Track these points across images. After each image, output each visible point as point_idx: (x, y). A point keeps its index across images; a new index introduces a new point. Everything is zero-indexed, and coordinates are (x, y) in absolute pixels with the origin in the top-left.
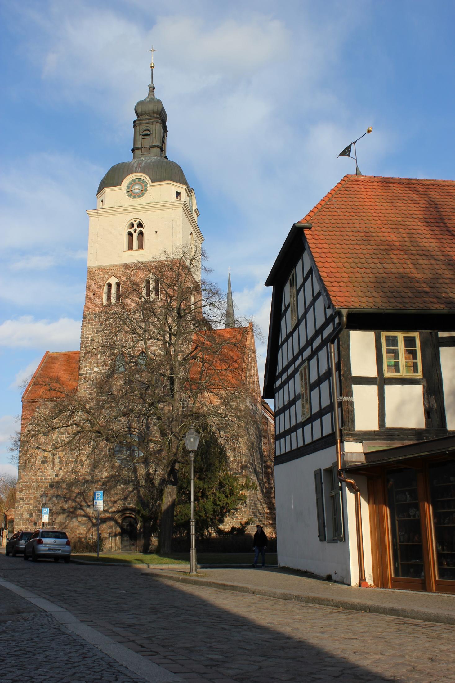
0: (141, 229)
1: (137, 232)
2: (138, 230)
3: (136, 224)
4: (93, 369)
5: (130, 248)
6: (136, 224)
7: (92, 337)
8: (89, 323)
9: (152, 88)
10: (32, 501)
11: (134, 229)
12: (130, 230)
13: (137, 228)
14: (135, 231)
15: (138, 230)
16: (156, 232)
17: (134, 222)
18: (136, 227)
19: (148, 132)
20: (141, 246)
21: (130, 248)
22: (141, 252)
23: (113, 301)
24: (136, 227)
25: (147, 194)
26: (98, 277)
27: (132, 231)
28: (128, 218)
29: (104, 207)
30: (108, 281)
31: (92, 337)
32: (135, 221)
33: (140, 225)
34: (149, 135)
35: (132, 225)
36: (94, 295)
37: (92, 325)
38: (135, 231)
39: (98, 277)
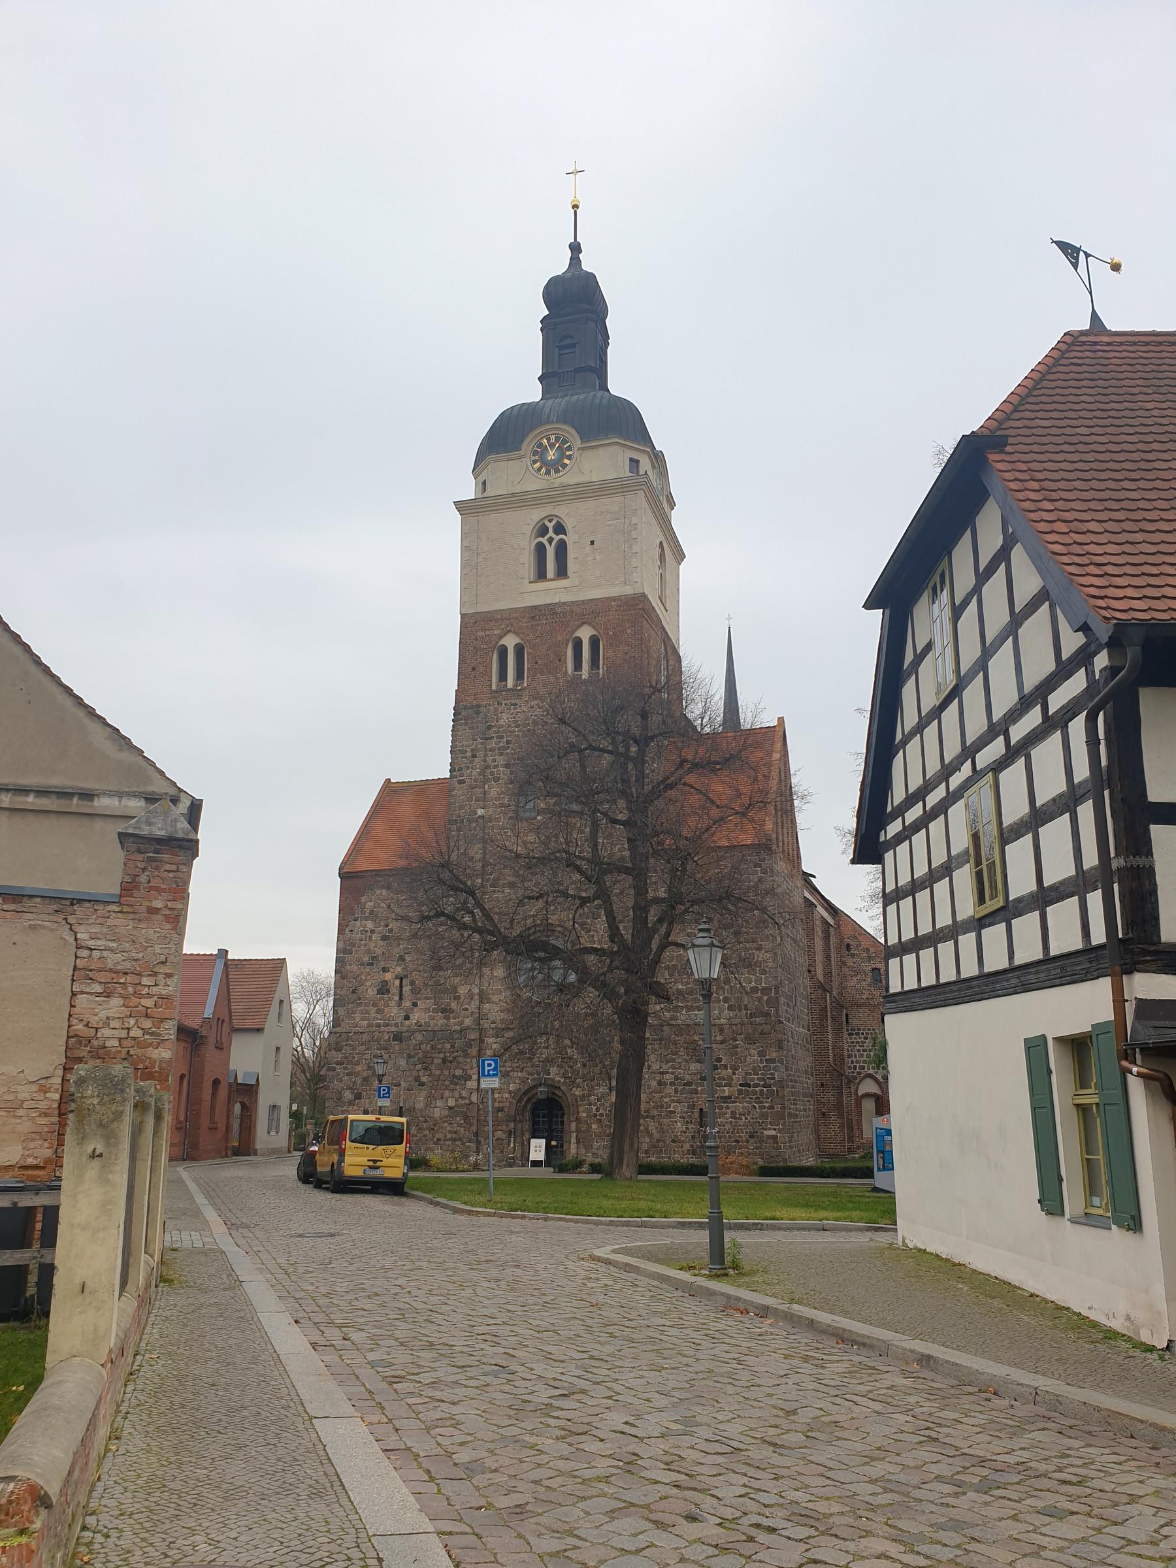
2: (557, 538)
3: (550, 526)
5: (541, 575)
6: (550, 526)
11: (547, 537)
12: (540, 539)
13: (554, 536)
14: (550, 540)
15: (557, 538)
16: (592, 543)
17: (547, 523)
18: (551, 533)
19: (568, 341)
20: (562, 572)
21: (541, 575)
22: (563, 583)
24: (551, 533)
26: (481, 633)
27: (544, 540)
28: (536, 515)
29: (486, 495)
30: (502, 642)
31: (472, 750)
32: (550, 521)
33: (560, 529)
34: (574, 346)
35: (543, 531)
36: (474, 669)
37: (473, 728)
38: (550, 540)
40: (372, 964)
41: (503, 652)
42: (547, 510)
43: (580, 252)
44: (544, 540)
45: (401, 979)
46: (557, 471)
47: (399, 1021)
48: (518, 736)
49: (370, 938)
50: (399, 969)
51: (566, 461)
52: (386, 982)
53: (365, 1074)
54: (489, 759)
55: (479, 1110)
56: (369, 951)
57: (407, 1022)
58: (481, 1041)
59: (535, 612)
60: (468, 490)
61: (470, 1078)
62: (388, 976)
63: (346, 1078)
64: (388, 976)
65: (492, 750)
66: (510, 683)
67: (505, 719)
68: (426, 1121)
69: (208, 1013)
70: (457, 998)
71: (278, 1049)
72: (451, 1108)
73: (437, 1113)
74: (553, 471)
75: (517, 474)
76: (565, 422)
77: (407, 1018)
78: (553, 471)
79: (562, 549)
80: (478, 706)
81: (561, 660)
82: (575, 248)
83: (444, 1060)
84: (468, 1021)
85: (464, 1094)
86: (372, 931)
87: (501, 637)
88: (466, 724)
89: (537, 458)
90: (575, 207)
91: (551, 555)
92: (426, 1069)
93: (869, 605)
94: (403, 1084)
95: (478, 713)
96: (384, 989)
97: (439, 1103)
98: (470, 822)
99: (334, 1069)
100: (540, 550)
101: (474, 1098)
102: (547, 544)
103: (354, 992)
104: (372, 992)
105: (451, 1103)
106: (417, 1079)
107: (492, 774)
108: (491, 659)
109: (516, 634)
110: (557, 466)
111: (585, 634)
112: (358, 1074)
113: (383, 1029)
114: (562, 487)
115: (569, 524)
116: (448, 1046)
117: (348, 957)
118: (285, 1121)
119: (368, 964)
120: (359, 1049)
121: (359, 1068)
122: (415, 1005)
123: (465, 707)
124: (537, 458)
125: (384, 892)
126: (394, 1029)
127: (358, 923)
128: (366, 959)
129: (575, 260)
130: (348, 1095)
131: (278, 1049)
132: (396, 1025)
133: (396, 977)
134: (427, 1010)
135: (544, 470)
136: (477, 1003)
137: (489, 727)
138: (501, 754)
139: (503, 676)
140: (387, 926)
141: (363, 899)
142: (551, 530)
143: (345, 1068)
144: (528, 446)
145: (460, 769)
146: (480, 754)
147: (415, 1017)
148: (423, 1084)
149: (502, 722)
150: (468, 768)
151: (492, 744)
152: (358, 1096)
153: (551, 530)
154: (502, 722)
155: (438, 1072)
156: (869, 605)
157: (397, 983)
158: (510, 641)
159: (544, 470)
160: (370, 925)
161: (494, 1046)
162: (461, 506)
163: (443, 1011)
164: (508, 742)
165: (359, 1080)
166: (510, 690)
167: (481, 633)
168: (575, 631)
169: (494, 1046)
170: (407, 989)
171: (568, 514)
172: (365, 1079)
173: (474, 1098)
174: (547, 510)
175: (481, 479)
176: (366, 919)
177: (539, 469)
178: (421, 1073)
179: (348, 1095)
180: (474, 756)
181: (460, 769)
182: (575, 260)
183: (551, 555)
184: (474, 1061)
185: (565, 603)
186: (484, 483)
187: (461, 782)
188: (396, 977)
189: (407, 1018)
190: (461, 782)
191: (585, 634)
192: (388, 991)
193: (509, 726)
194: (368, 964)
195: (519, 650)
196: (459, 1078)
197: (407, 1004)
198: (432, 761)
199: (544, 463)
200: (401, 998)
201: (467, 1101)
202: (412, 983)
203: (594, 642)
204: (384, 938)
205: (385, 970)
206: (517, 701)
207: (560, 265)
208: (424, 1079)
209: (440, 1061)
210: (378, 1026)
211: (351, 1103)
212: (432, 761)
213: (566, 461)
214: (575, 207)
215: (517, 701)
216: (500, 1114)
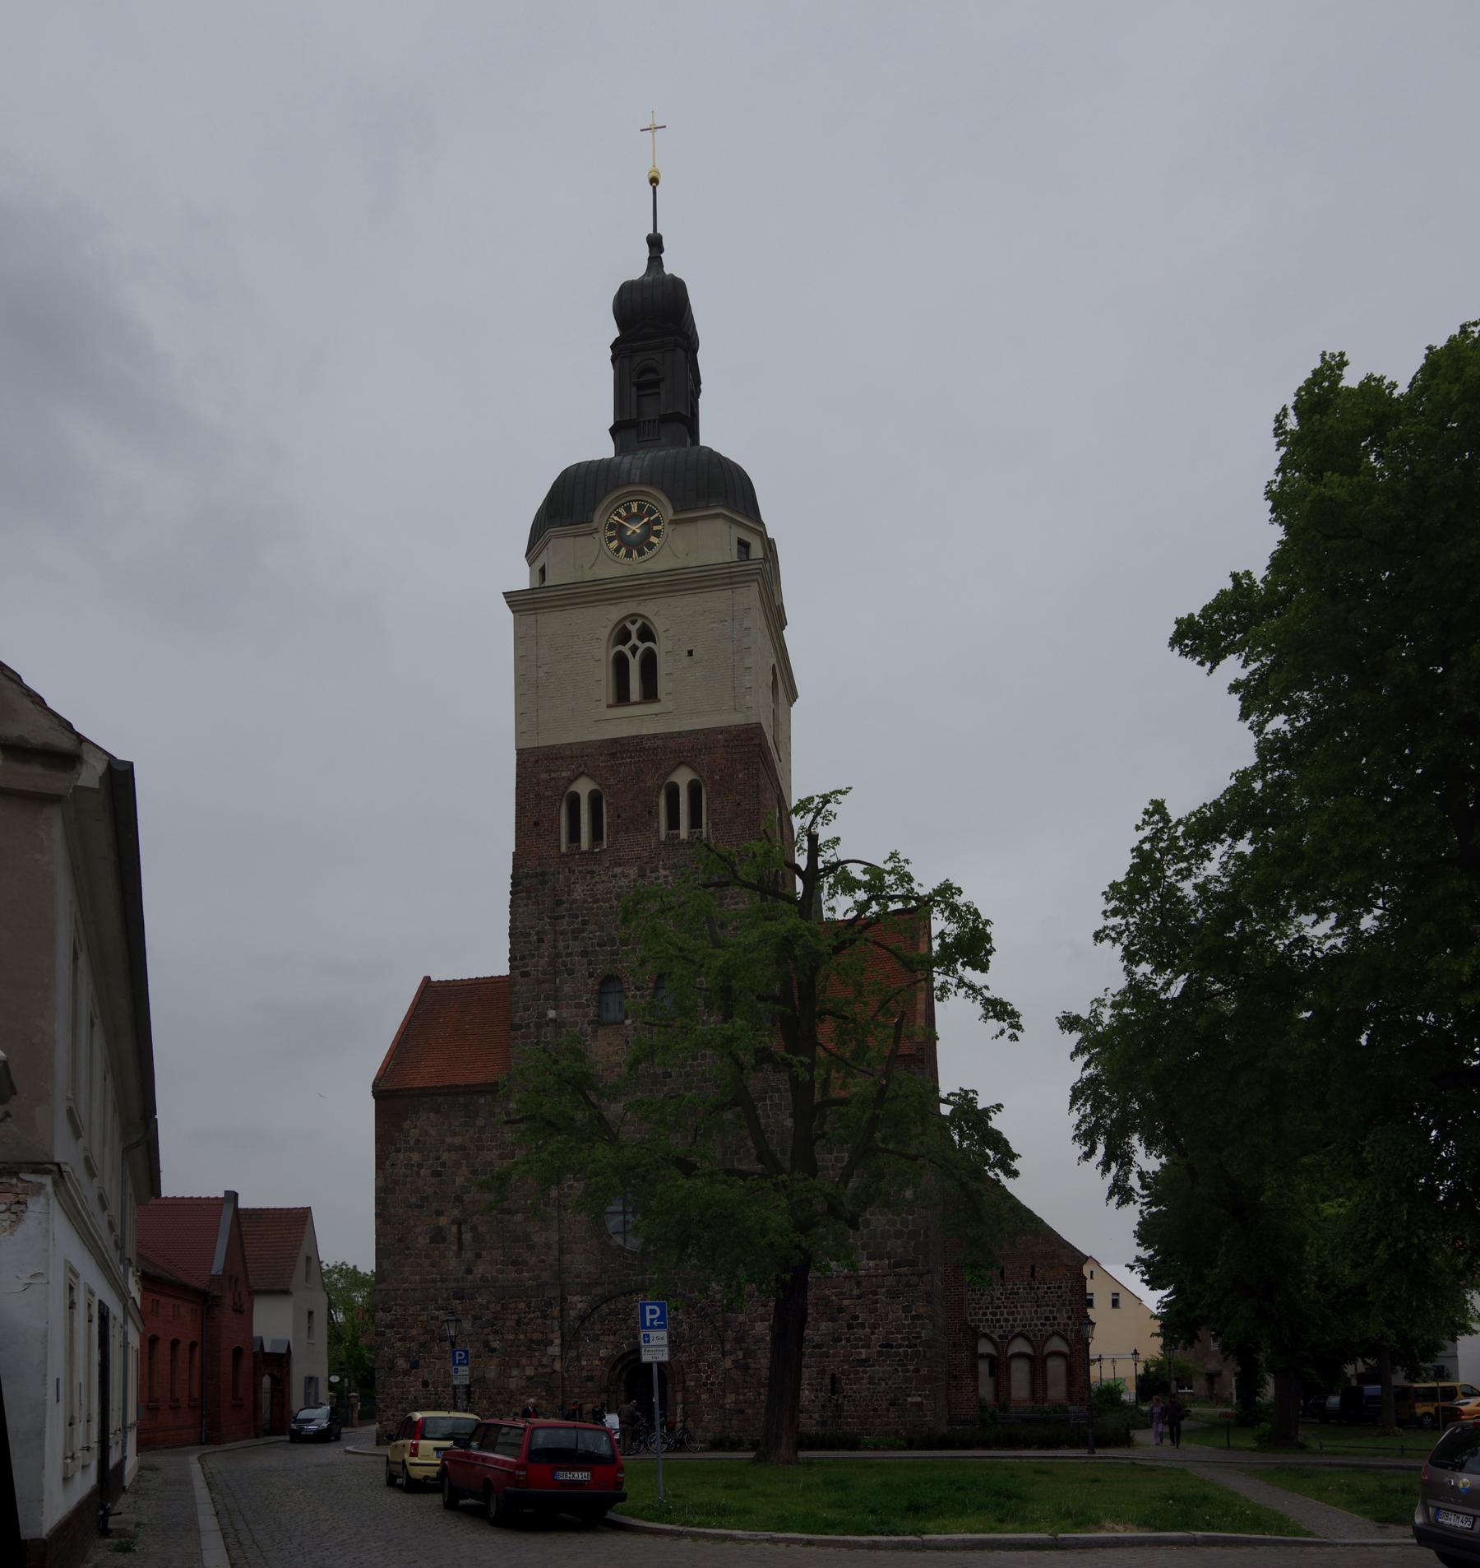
1: (639, 653)
2: (642, 646)
3: (634, 629)
4: (545, 1015)
5: (622, 696)
6: (634, 629)
9: (655, 244)
10: (414, 1332)
11: (629, 644)
12: (620, 648)
13: (638, 643)
14: (634, 650)
15: (642, 646)
17: (629, 626)
18: (634, 640)
20: (650, 693)
23: (585, 843)
24: (634, 640)
26: (544, 776)
27: (625, 649)
28: (615, 613)
31: (538, 933)
32: (633, 623)
33: (646, 634)
35: (623, 636)
36: (536, 824)
38: (634, 650)
40: (421, 1207)
41: (574, 802)
42: (630, 607)
43: (662, 250)
44: (625, 649)
45: (460, 1225)
48: (597, 915)
49: (418, 1173)
50: (456, 1212)
51: (653, 539)
52: (441, 1228)
53: (422, 1338)
54: (561, 945)
55: (564, 1379)
57: (470, 1277)
58: (564, 1299)
59: (616, 748)
60: (522, 579)
61: (551, 1343)
62: (443, 1221)
63: (399, 1344)
64: (443, 1221)
65: (563, 933)
66: (585, 843)
68: (499, 1393)
69: (218, 1267)
70: (531, 1247)
71: (311, 1314)
72: (529, 1378)
73: (513, 1384)
74: (635, 553)
75: (587, 556)
76: (651, 484)
77: (469, 1271)
78: (635, 553)
80: (544, 874)
81: (652, 813)
82: (655, 244)
83: (518, 1322)
84: (545, 1276)
85: (545, 1361)
87: (571, 781)
88: (529, 898)
89: (613, 533)
90: (654, 181)
91: (635, 671)
92: (496, 1332)
95: (544, 883)
96: (438, 1236)
97: (515, 1372)
98: (538, 1026)
99: (382, 1334)
100: (621, 663)
101: (557, 1366)
102: (629, 654)
103: (400, 1240)
104: (423, 1241)
105: (530, 1372)
106: (486, 1344)
107: (565, 964)
108: (559, 811)
109: (592, 777)
110: (640, 545)
111: (683, 778)
112: (413, 1339)
115: (659, 626)
116: (522, 1305)
118: (324, 1394)
119: (417, 1206)
121: (414, 1332)
122: (478, 1255)
123: (527, 876)
124: (613, 533)
125: (432, 1115)
126: (453, 1284)
127: (401, 1155)
128: (413, 1200)
129: (655, 260)
130: (402, 1363)
131: (311, 1314)
133: (454, 1222)
135: (623, 550)
136: (556, 1253)
137: (559, 903)
138: (575, 939)
139: (574, 836)
140: (438, 1158)
141: (407, 1125)
142: (634, 635)
143: (397, 1333)
144: (599, 519)
145: (523, 958)
147: (480, 1269)
148: (493, 1350)
149: (576, 896)
150: (533, 956)
151: (564, 925)
152: (415, 1365)
153: (634, 635)
154: (576, 896)
155: (511, 1337)
157: (454, 1229)
158: (583, 788)
159: (623, 550)
160: (416, 1157)
161: (580, 1305)
162: (514, 600)
163: (515, 1263)
164: (585, 923)
165: (414, 1346)
166: (584, 853)
167: (544, 776)
168: (669, 774)
169: (580, 1305)
170: (467, 1237)
172: (422, 1345)
173: (557, 1366)
174: (630, 607)
175: (538, 565)
176: (411, 1149)
177: (617, 550)
178: (491, 1337)
179: (402, 1363)
180: (541, 940)
181: (523, 958)
182: (655, 260)
183: (635, 671)
184: (556, 1323)
185: (655, 736)
186: (543, 571)
188: (454, 1222)
189: (469, 1271)
191: (683, 778)
192: (444, 1240)
193: (585, 901)
194: (417, 1206)
195: (595, 799)
196: (538, 1343)
197: (468, 1255)
198: (485, 953)
199: (624, 541)
200: (460, 1248)
201: (549, 1370)
202: (474, 1229)
203: (695, 790)
204: (436, 1174)
205: (439, 1213)
206: (595, 868)
207: (636, 268)
208: (496, 1344)
209: (513, 1323)
210: (434, 1281)
211: (406, 1373)
212: (485, 953)
213: (653, 539)
214: (654, 181)
215: (595, 868)
216: (589, 1384)
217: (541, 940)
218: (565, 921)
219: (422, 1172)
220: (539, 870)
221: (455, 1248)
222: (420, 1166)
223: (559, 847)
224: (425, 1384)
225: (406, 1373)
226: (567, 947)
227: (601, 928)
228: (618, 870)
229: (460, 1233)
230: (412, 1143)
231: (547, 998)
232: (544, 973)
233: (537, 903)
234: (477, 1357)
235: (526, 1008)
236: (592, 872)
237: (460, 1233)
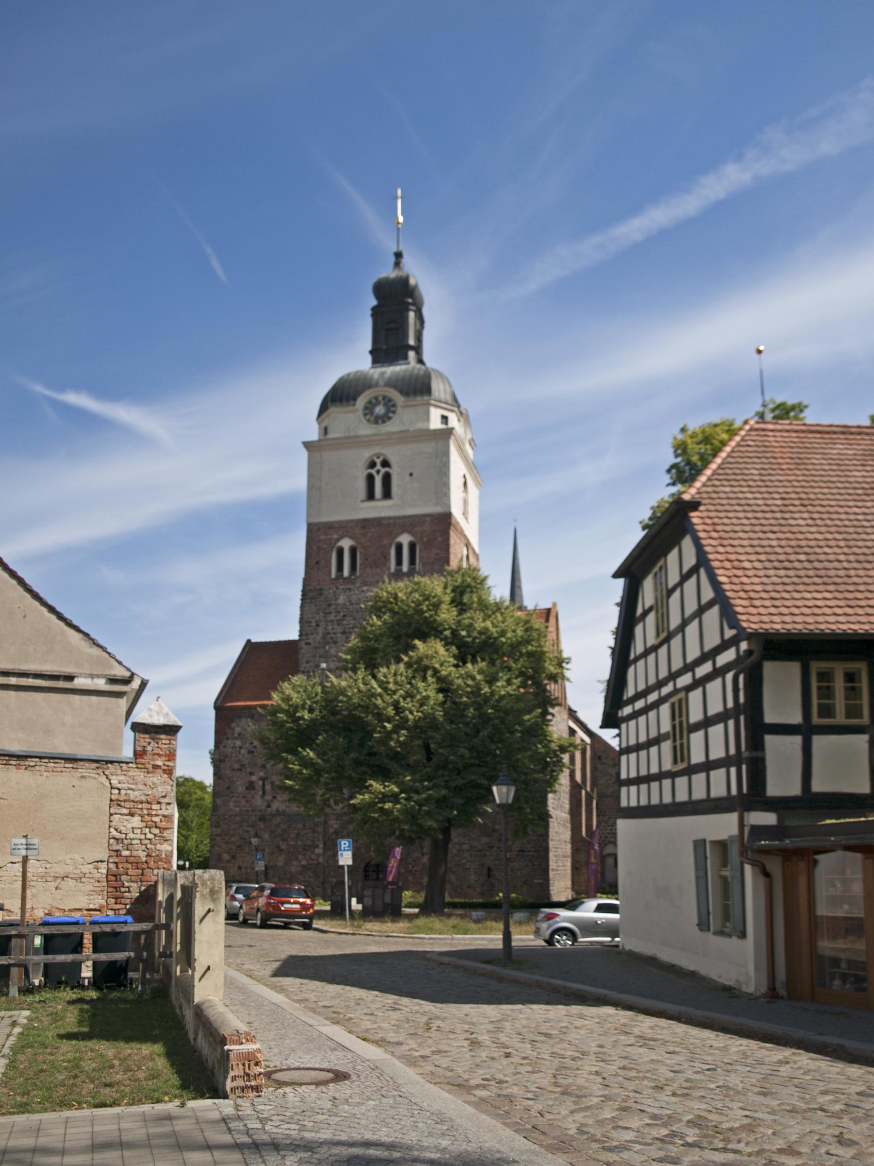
0: (387, 469)
5: (371, 496)
7: (316, 621)
8: (311, 603)
10: (234, 839)
14: (378, 472)
18: (378, 467)
21: (371, 496)
23: (346, 572)
24: (378, 467)
25: (396, 418)
27: (373, 471)
31: (316, 621)
32: (378, 458)
33: (386, 464)
35: (372, 465)
36: (317, 563)
38: (378, 472)
39: (323, 537)
40: (240, 770)
41: (340, 552)
44: (373, 471)
46: (384, 422)
47: (263, 808)
49: (239, 752)
53: (238, 843)
54: (330, 628)
56: (238, 761)
57: (269, 810)
59: (366, 523)
62: (254, 778)
64: (254, 778)
65: (332, 621)
66: (346, 572)
67: (341, 600)
79: (387, 480)
80: (321, 589)
86: (241, 748)
87: (338, 540)
91: (379, 482)
92: (284, 840)
93: (616, 575)
94: (267, 850)
95: (321, 594)
96: (251, 786)
100: (370, 479)
103: (228, 788)
104: (241, 789)
106: (278, 847)
109: (351, 538)
110: (384, 419)
113: (250, 813)
114: (388, 434)
117: (222, 765)
120: (233, 826)
121: (234, 839)
122: (275, 797)
123: (311, 590)
127: (230, 742)
128: (236, 766)
130: (226, 857)
132: (261, 811)
134: (283, 802)
137: (330, 605)
138: (339, 624)
140: (252, 743)
141: (233, 725)
145: (307, 635)
146: (322, 624)
147: (275, 806)
150: (312, 634)
151: (332, 617)
152: (234, 857)
155: (292, 843)
156: (616, 575)
157: (261, 783)
160: (238, 743)
165: (234, 847)
166: (345, 579)
170: (268, 787)
171: (391, 453)
172: (239, 846)
176: (236, 738)
179: (226, 857)
180: (318, 625)
181: (307, 635)
183: (379, 482)
187: (308, 644)
189: (269, 806)
190: (308, 644)
192: (254, 788)
193: (345, 604)
197: (268, 797)
202: (272, 783)
204: (250, 752)
205: (251, 774)
206: (351, 586)
210: (247, 811)
217: (318, 625)
218: (333, 615)
219: (242, 751)
220: (318, 587)
221: (261, 793)
222: (241, 748)
223: (330, 575)
224: (240, 868)
225: (228, 862)
226: (333, 629)
227: (354, 619)
228: (365, 588)
229: (264, 785)
230: (236, 735)
231: (321, 657)
232: (319, 643)
233: (316, 605)
234: (272, 853)
235: (308, 662)
236: (350, 589)
237: (264, 785)
